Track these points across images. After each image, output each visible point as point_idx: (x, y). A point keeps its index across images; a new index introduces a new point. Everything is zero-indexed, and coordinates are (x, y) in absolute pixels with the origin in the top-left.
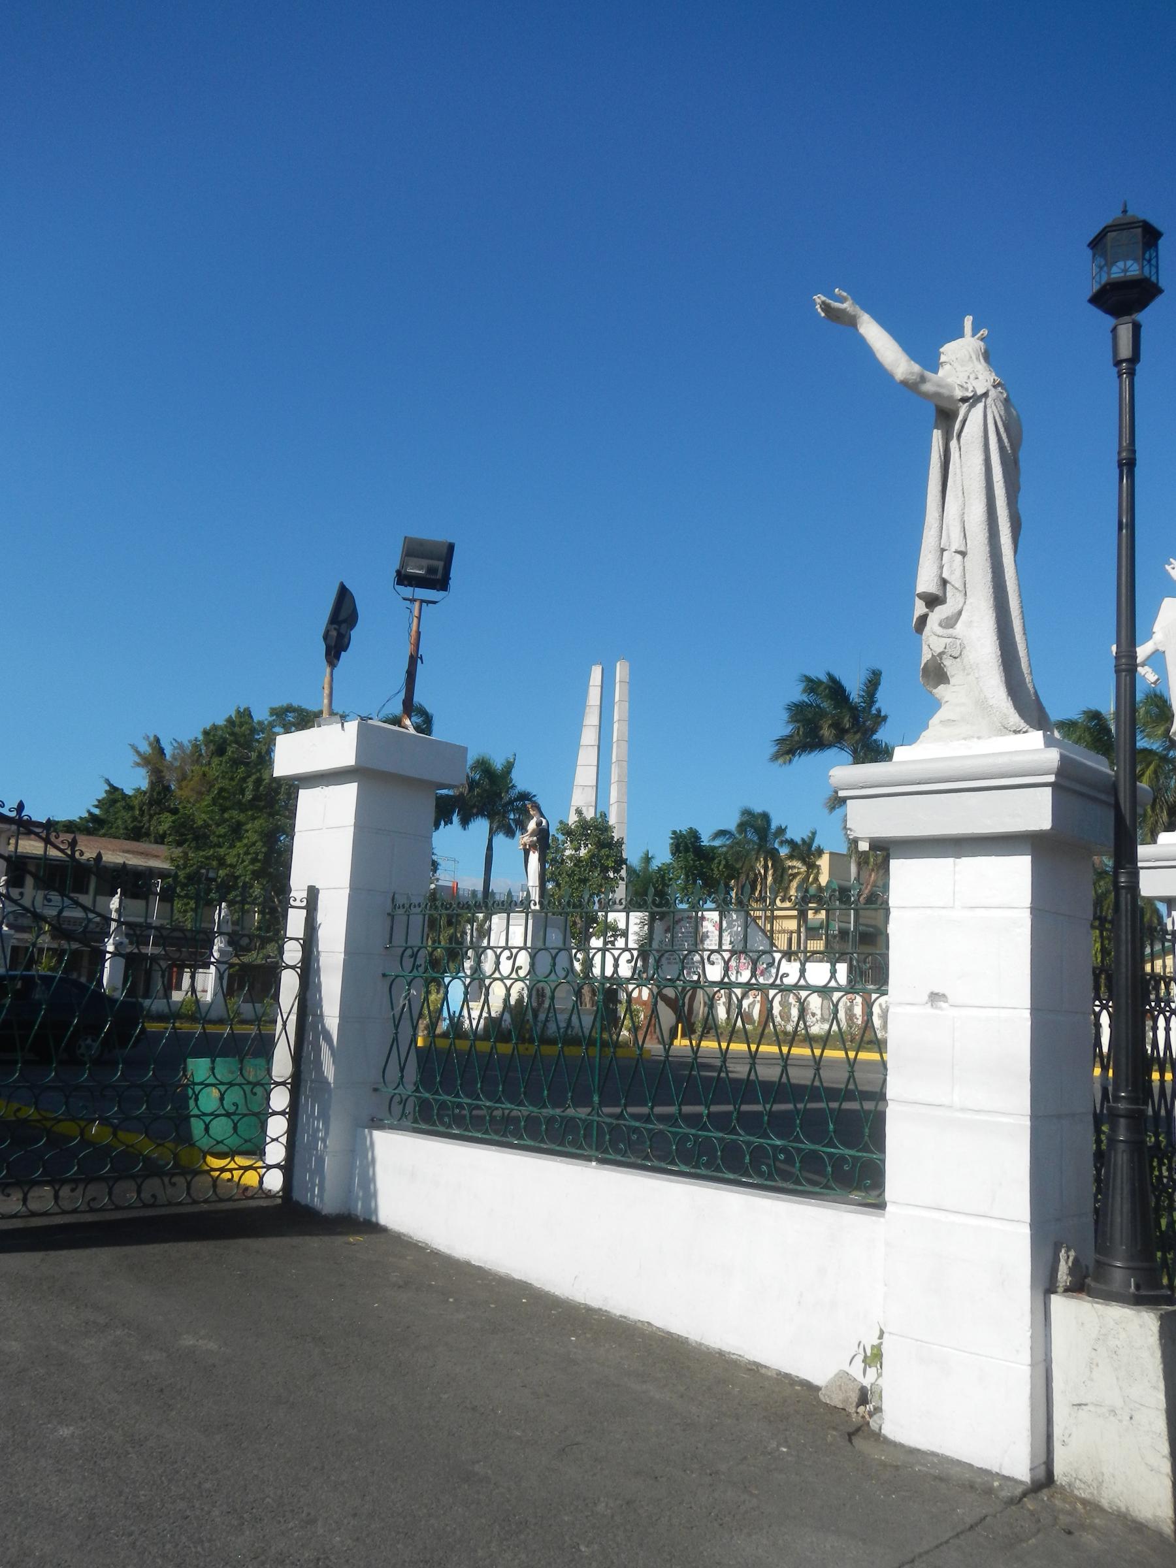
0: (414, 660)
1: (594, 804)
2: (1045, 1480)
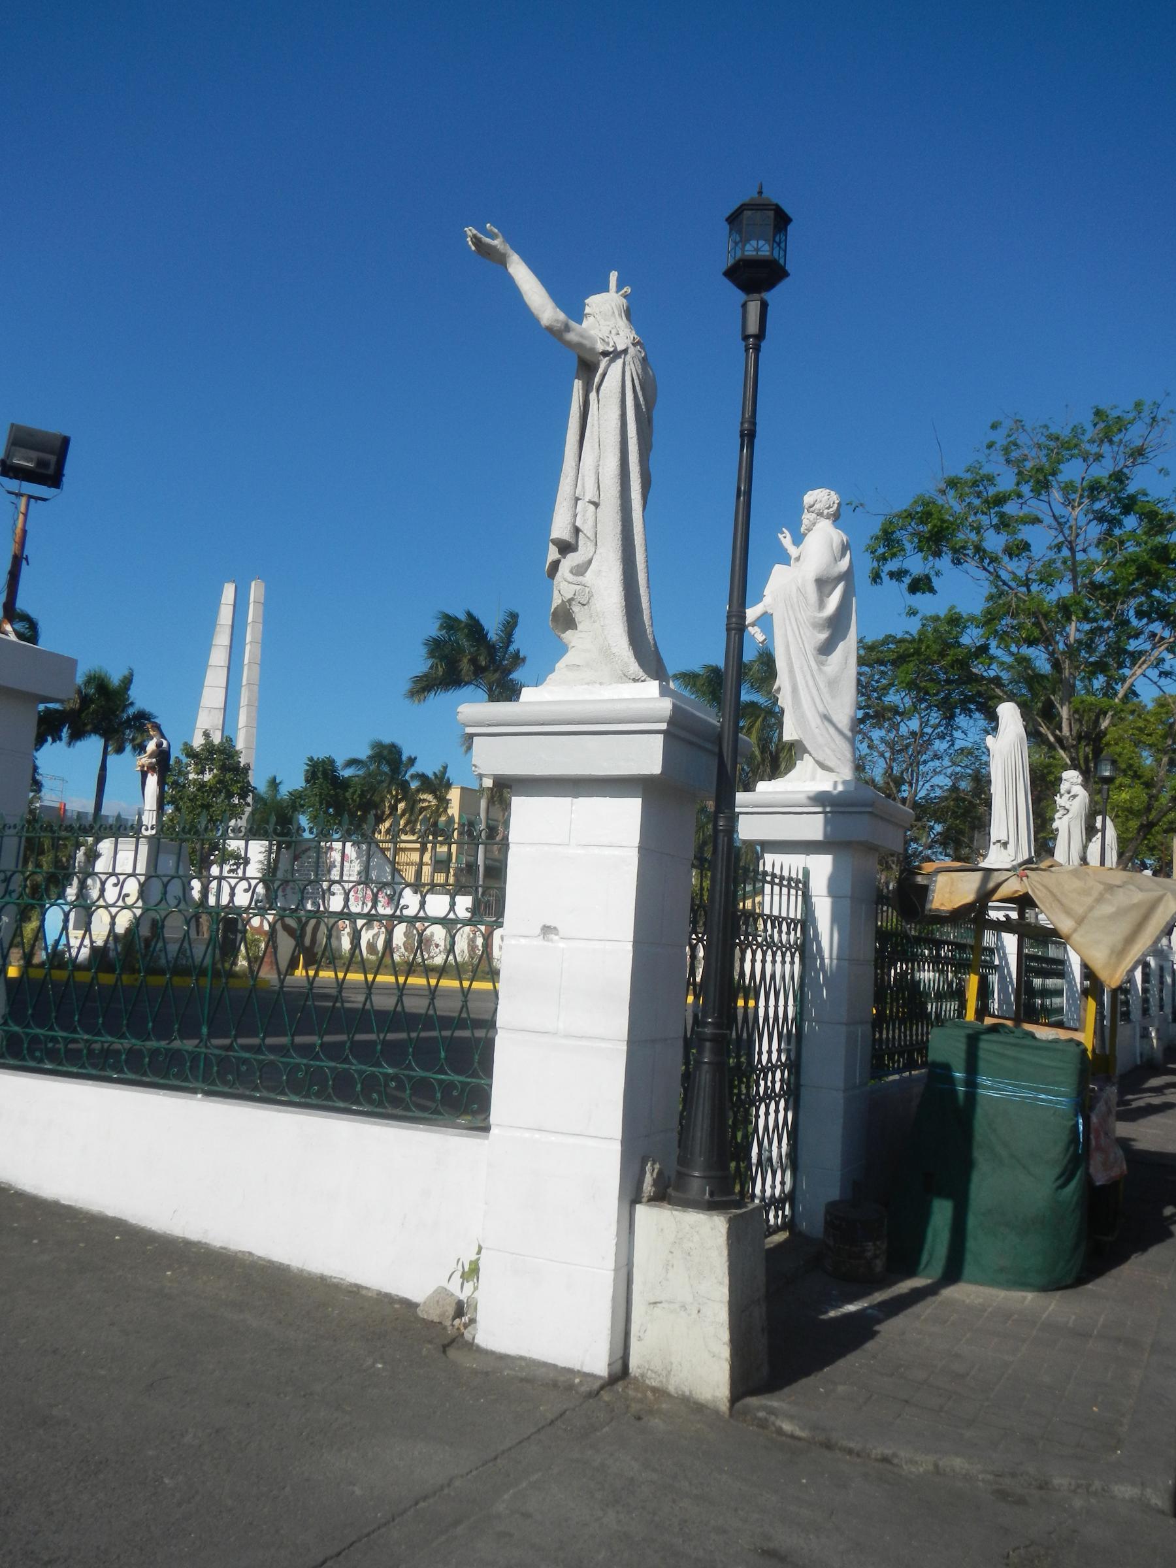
0: (18, 561)
1: (221, 728)
2: (621, 1372)
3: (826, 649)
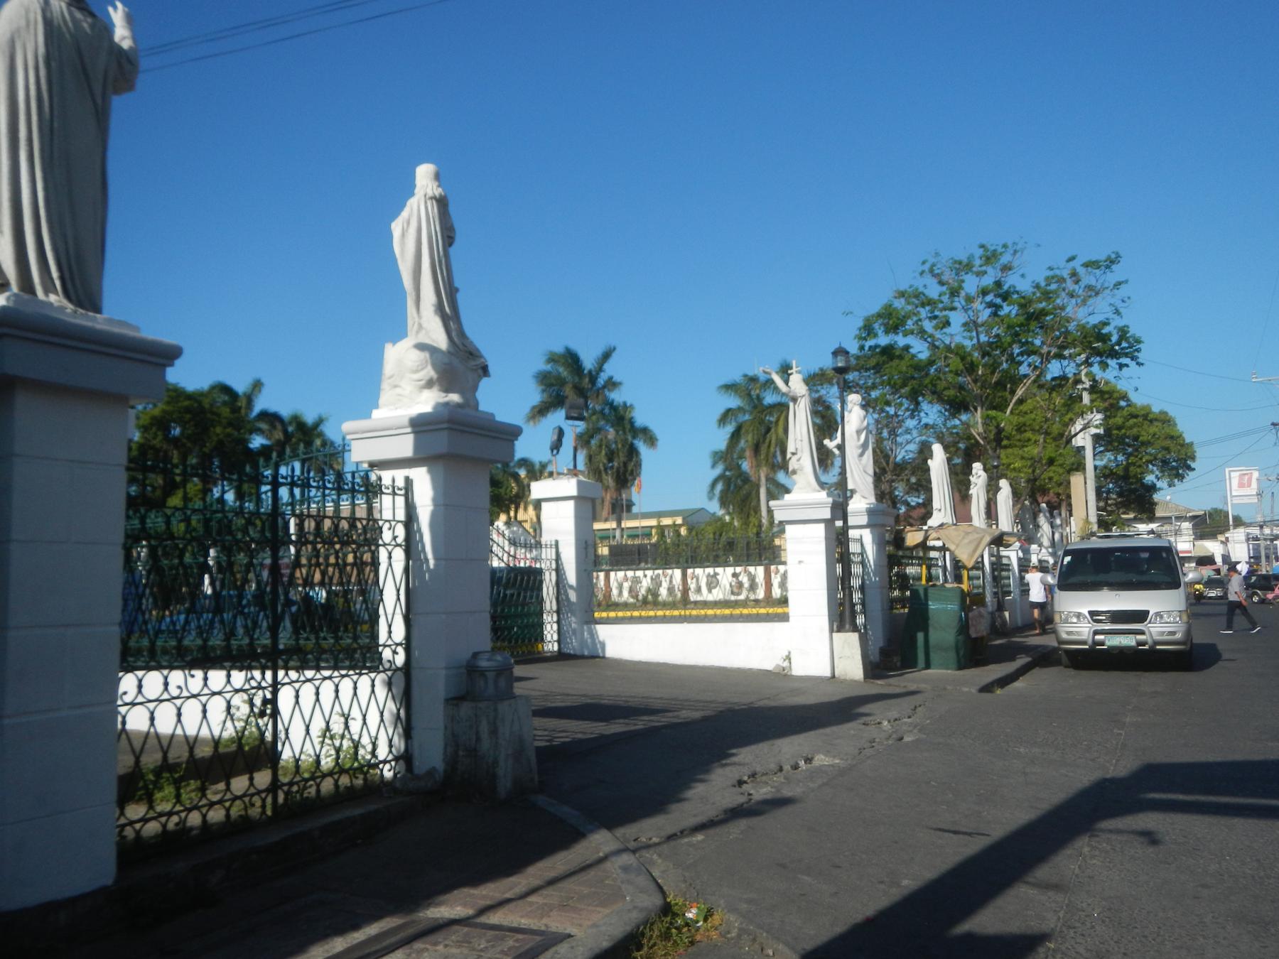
2: (833, 676)
3: (861, 455)
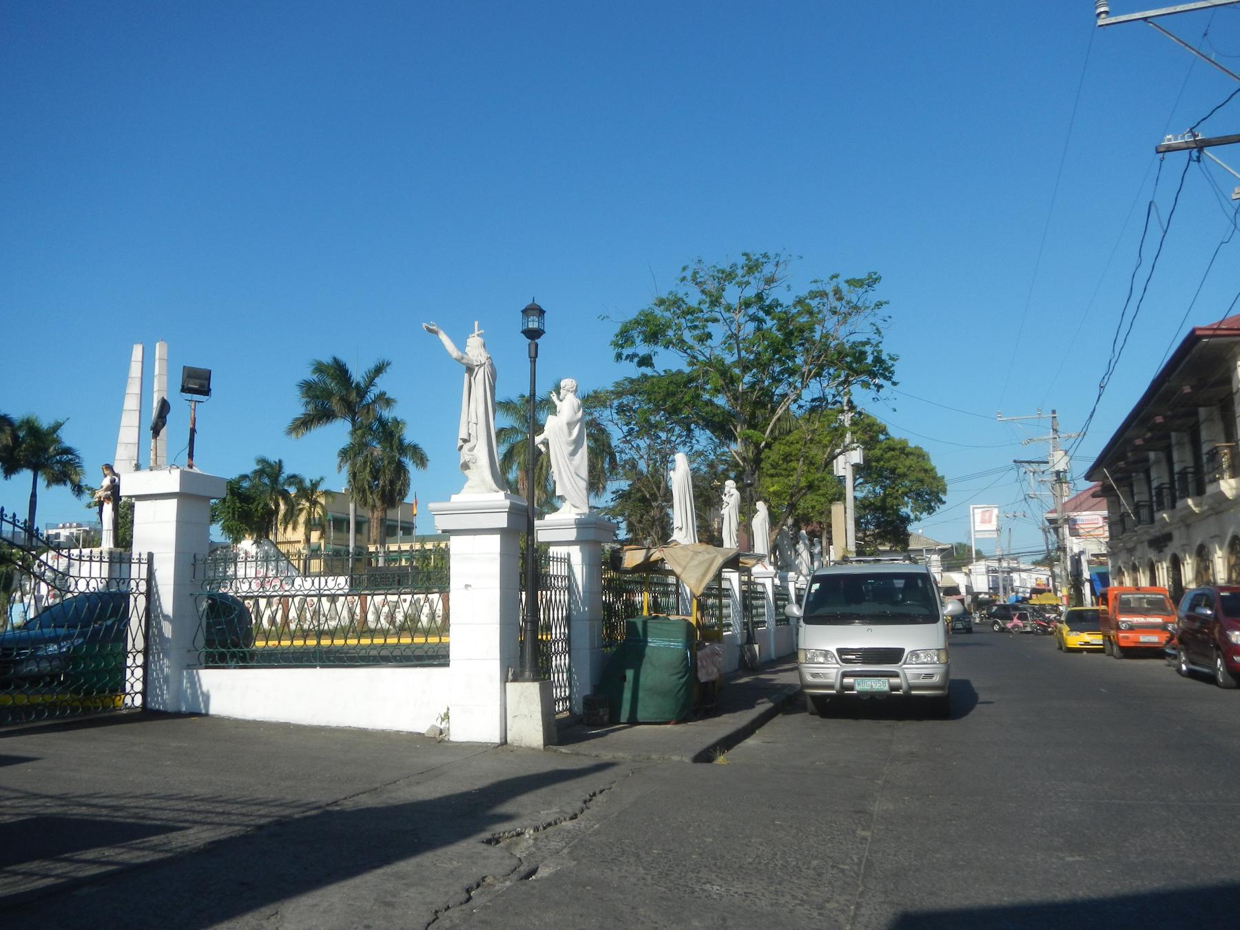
0: (193, 431)
2: (504, 742)
3: (573, 453)
